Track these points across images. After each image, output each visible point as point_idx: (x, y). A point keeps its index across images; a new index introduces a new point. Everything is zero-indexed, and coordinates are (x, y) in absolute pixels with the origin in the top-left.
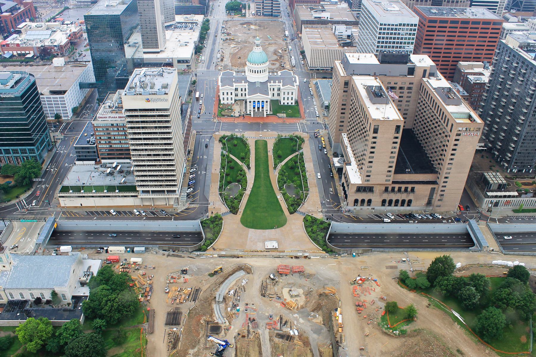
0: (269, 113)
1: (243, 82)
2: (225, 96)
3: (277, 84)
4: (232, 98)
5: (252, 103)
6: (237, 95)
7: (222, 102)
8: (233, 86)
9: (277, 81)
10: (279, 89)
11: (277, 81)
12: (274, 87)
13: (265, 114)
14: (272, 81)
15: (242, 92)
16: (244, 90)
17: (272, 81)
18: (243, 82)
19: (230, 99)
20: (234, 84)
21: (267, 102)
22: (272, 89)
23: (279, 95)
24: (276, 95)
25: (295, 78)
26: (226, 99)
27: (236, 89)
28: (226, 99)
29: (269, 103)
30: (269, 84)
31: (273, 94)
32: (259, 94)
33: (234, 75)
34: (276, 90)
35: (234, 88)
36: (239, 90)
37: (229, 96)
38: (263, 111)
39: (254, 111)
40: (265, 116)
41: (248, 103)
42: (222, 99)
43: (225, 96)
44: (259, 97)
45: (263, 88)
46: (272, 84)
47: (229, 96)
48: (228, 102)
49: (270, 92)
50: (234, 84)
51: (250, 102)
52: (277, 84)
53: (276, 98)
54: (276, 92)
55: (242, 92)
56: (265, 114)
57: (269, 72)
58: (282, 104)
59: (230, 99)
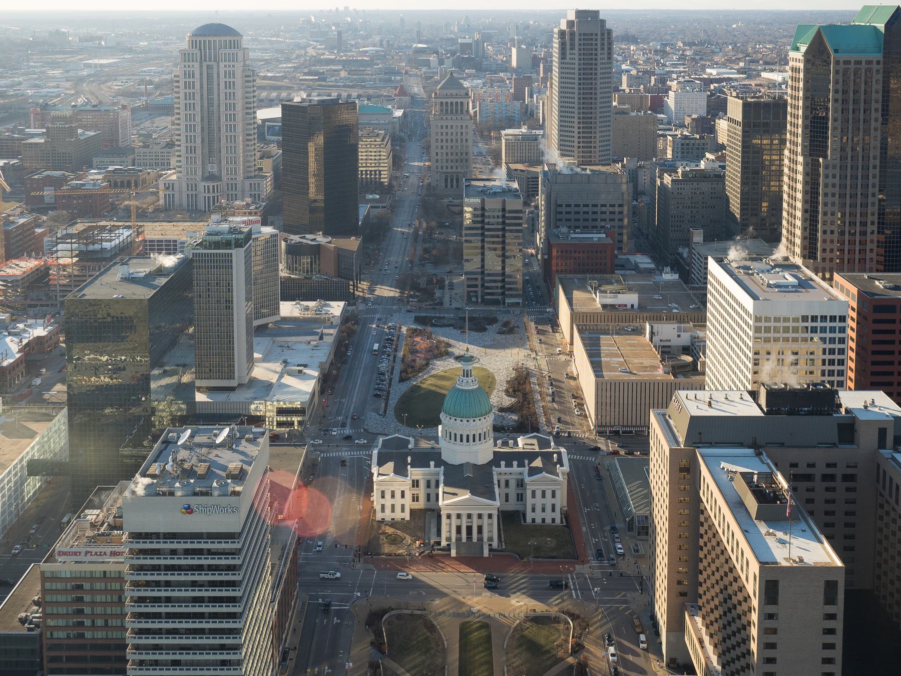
1: (432, 463)
4: (403, 506)
5: (454, 518)
9: (515, 463)
11: (515, 463)
12: (507, 477)
14: (503, 463)
16: (433, 484)
17: (503, 463)
18: (432, 463)
19: (398, 508)
21: (490, 516)
22: (503, 484)
23: (520, 497)
24: (513, 497)
31: (507, 495)
34: (513, 484)
37: (398, 501)
38: (480, 539)
39: (459, 540)
40: (486, 553)
41: (444, 518)
45: (476, 479)
47: (398, 501)
48: (393, 515)
51: (449, 516)
53: (513, 505)
54: (513, 491)
59: (398, 508)
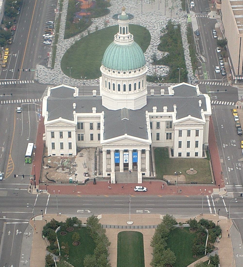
0: (147, 175)
1: (94, 109)
2: (57, 140)
3: (165, 113)
4: (70, 144)
5: (112, 154)
6: (80, 138)
7: (50, 152)
8: (72, 119)
9: (165, 108)
10: (170, 125)
11: (165, 108)
12: (158, 120)
13: (140, 176)
14: (155, 108)
15: (92, 132)
16: (95, 126)
17: (155, 108)
18: (94, 109)
19: (66, 146)
20: (76, 115)
21: (143, 152)
22: (155, 125)
23: (169, 136)
24: (163, 136)
25: (204, 100)
26: (57, 146)
27: (80, 126)
28: (57, 146)
29: (147, 153)
30: (148, 114)
32: (126, 135)
33: (76, 94)
34: (163, 125)
35: (75, 122)
36: (87, 126)
37: (66, 140)
39: (117, 170)
41: (104, 154)
42: (49, 145)
43: (57, 140)
44: (127, 141)
46: (155, 113)
47: (66, 140)
48: (62, 152)
49: (149, 131)
50: (76, 115)
52: (165, 113)
53: (163, 143)
54: (163, 131)
55: (92, 132)
56: (140, 176)
57: (149, 89)
58: (176, 155)
59: (66, 146)
